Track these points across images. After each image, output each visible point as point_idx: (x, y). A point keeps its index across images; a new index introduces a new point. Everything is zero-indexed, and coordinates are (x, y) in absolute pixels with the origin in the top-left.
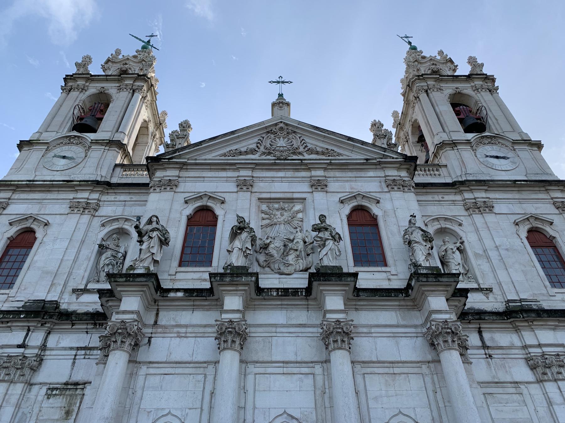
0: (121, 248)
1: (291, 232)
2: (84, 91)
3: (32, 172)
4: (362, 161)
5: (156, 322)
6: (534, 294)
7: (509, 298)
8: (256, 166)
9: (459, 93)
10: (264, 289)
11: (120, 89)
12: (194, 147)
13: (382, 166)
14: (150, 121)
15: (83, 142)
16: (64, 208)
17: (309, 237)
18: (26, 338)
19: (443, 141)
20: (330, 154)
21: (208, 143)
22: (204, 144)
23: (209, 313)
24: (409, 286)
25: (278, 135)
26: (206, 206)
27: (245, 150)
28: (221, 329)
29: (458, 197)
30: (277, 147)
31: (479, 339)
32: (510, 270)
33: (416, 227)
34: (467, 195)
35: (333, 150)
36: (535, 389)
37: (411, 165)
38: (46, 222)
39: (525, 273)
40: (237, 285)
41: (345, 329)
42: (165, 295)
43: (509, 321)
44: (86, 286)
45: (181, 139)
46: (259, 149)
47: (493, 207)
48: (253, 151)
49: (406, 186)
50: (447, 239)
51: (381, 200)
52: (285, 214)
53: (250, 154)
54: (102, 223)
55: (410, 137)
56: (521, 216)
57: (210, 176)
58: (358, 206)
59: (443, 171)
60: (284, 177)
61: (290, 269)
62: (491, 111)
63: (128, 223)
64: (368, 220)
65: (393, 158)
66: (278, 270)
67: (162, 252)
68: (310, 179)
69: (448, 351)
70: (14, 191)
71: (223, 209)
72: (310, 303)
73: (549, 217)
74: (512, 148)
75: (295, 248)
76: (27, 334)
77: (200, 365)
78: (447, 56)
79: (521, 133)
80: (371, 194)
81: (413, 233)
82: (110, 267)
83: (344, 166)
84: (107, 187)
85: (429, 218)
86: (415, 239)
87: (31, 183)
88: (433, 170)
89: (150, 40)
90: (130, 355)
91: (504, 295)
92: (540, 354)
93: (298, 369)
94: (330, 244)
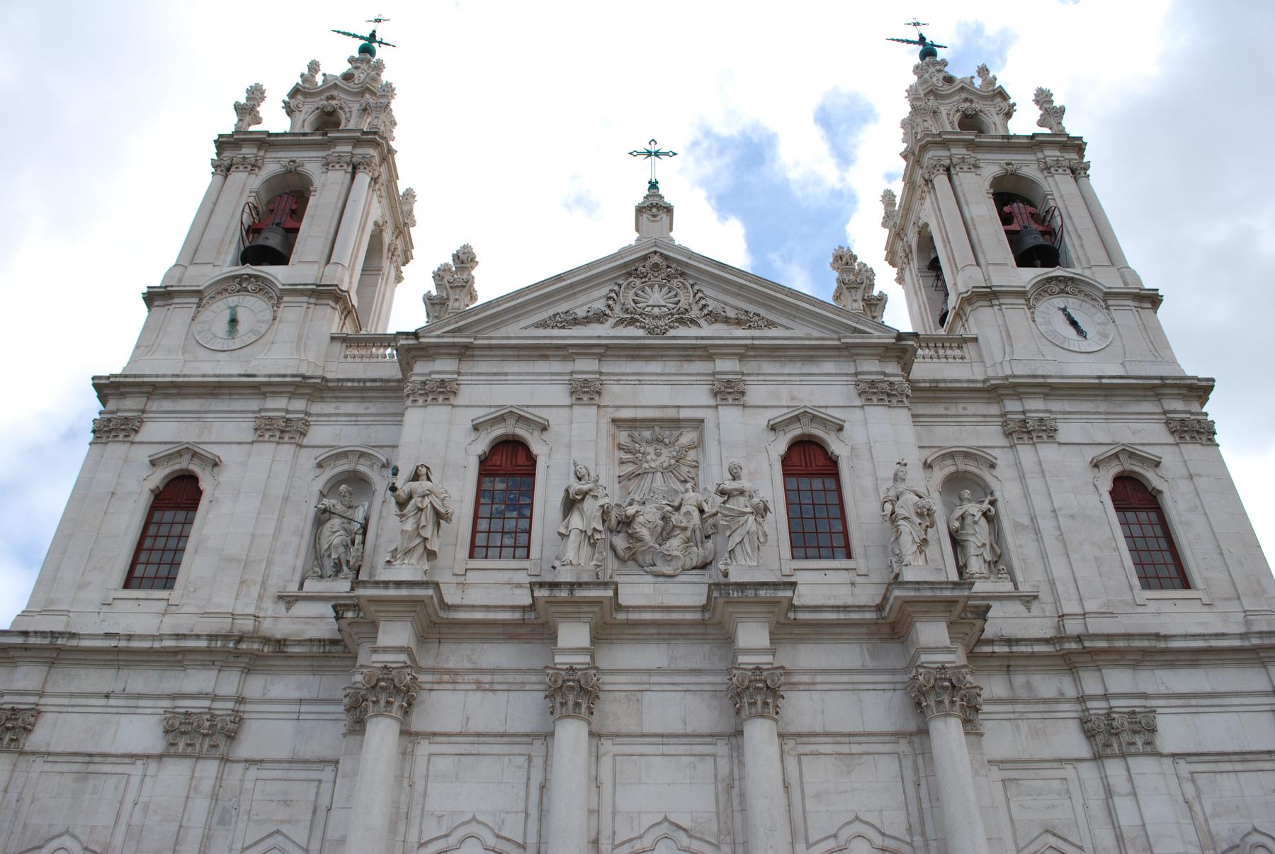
2: (257, 170)
3: (177, 355)
8: (605, 351)
9: (1012, 174)
10: (628, 607)
11: (328, 164)
14: (386, 222)
16: (243, 429)
20: (752, 324)
23: (528, 646)
25: (649, 279)
27: (584, 315)
28: (555, 682)
29: (994, 409)
30: (648, 306)
32: (1073, 556)
34: (1012, 405)
35: (759, 315)
36: (1088, 772)
39: (1098, 561)
41: (769, 683)
45: (458, 290)
46: (612, 310)
47: (1056, 430)
48: (600, 318)
49: (895, 395)
50: (967, 493)
51: (846, 425)
52: (665, 451)
54: (318, 460)
59: (970, 350)
60: (662, 374)
62: (1071, 218)
64: (821, 464)
66: (652, 566)
67: (440, 534)
68: (712, 378)
70: (149, 395)
73: (1155, 451)
74: (1102, 304)
75: (683, 525)
77: (519, 739)
78: (996, 79)
83: (776, 352)
85: (936, 452)
89: (374, 31)
90: (402, 724)
91: (1058, 604)
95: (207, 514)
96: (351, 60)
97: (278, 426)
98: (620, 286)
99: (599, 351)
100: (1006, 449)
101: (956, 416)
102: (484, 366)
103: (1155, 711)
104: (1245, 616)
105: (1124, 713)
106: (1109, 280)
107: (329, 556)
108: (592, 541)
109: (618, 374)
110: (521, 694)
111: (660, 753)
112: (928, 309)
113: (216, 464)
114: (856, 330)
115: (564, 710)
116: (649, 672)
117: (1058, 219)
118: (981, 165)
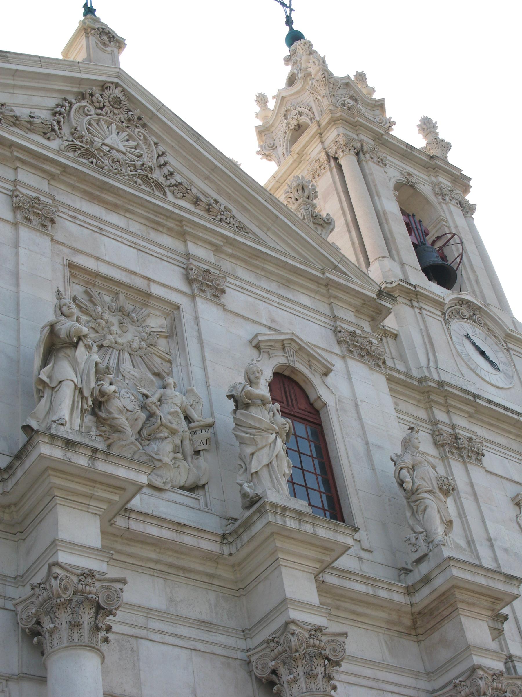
20: (224, 218)
25: (106, 113)
35: (229, 210)
65: (355, 283)
81: (416, 468)
99: (52, 170)
109: (75, 210)
115: (76, 636)
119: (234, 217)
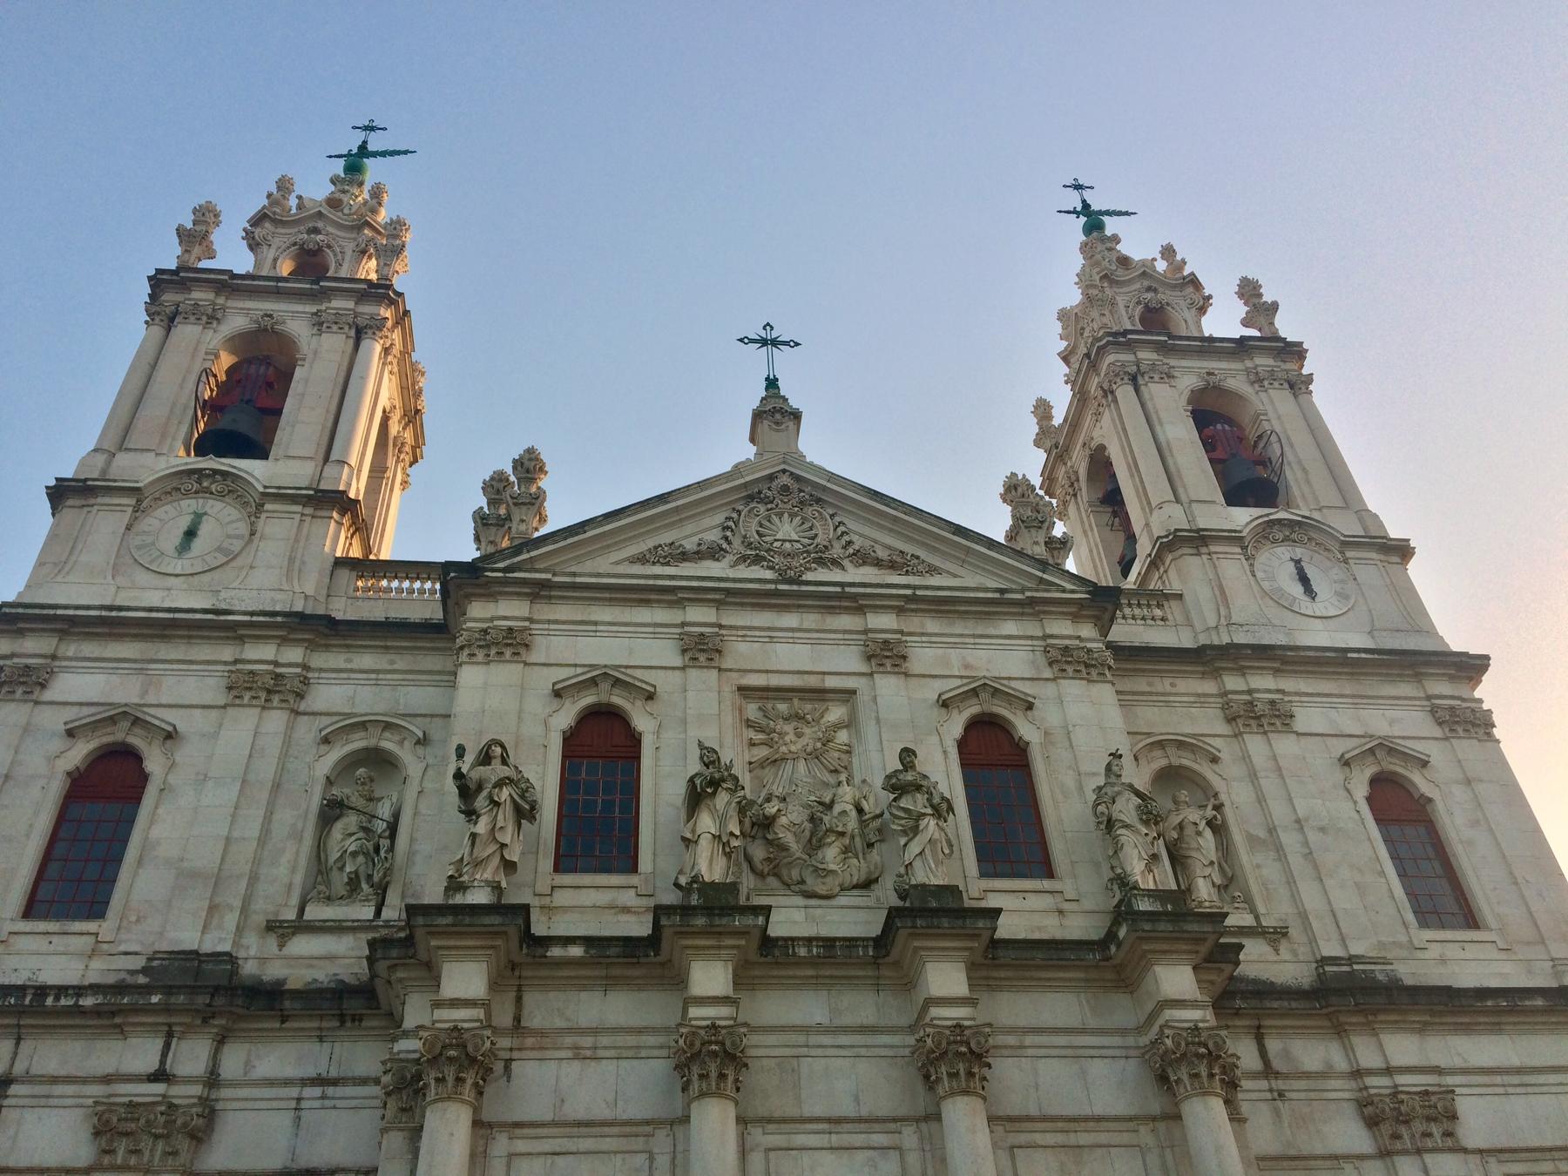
0: (380, 804)
1: (824, 782)
2: (215, 323)
3: (105, 578)
4: (990, 595)
5: (517, 1019)
6: (1382, 945)
7: (1326, 953)
8: (729, 596)
9: (1214, 387)
10: (778, 939)
11: (321, 324)
12: (565, 539)
13: (1037, 608)
14: (395, 407)
15: (238, 491)
17: (872, 800)
18: (164, 1055)
19: (1177, 530)
20: (910, 569)
21: (602, 526)
22: (595, 528)
23: (643, 995)
24: (1111, 936)
26: (610, 705)
27: (695, 548)
28: (692, 1045)
29: (1209, 687)
30: (776, 540)
31: (1256, 1053)
32: (1329, 882)
33: (1123, 784)
34: (1232, 682)
35: (918, 558)
37: (1106, 609)
38: (170, 729)
40: (720, 933)
41: (973, 1045)
42: (540, 951)
43: (1325, 1011)
44: (301, 911)
45: (524, 508)
46: (729, 543)
47: (1292, 716)
48: (714, 553)
49: (1094, 666)
50: (1184, 795)
52: (807, 731)
53: (707, 559)
54: (323, 733)
55: (1083, 483)
56: (1357, 741)
57: (608, 618)
58: (983, 714)
59: (1173, 610)
61: (831, 884)
62: (1292, 446)
63: (392, 734)
67: (521, 838)
68: (863, 637)
69: (1200, 1098)
71: (652, 714)
72: (885, 972)
73: (1419, 746)
74: (1339, 556)
75: (840, 829)
76: (167, 1046)
77: (634, 1129)
78: (1185, 263)
79: (1363, 514)
80: (1013, 684)
82: (361, 859)
83: (944, 606)
84: (327, 631)
86: (1123, 817)
87: (114, 614)
88: (1149, 606)
92: (1388, 1091)
93: (863, 1136)
94: (930, 825)
95: (156, 808)
96: (334, 181)
97: (263, 683)
98: (739, 512)
99: (717, 597)
100: (1228, 739)
101: (1163, 694)
102: (564, 611)
103: (1453, 1092)
104: (1554, 966)
105: (1415, 1093)
106: (1346, 526)
107: (341, 869)
108: (728, 850)
109: (743, 628)
110: (635, 1062)
111: (827, 1145)
112: (1103, 556)
113: (171, 736)
114: (1041, 580)
116: (805, 1030)
117: (1276, 447)
118: (1176, 374)
119: (923, 561)
